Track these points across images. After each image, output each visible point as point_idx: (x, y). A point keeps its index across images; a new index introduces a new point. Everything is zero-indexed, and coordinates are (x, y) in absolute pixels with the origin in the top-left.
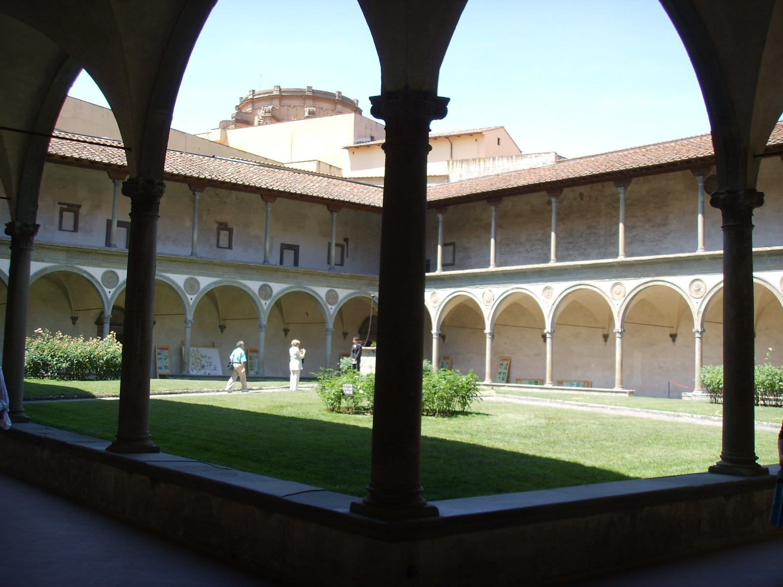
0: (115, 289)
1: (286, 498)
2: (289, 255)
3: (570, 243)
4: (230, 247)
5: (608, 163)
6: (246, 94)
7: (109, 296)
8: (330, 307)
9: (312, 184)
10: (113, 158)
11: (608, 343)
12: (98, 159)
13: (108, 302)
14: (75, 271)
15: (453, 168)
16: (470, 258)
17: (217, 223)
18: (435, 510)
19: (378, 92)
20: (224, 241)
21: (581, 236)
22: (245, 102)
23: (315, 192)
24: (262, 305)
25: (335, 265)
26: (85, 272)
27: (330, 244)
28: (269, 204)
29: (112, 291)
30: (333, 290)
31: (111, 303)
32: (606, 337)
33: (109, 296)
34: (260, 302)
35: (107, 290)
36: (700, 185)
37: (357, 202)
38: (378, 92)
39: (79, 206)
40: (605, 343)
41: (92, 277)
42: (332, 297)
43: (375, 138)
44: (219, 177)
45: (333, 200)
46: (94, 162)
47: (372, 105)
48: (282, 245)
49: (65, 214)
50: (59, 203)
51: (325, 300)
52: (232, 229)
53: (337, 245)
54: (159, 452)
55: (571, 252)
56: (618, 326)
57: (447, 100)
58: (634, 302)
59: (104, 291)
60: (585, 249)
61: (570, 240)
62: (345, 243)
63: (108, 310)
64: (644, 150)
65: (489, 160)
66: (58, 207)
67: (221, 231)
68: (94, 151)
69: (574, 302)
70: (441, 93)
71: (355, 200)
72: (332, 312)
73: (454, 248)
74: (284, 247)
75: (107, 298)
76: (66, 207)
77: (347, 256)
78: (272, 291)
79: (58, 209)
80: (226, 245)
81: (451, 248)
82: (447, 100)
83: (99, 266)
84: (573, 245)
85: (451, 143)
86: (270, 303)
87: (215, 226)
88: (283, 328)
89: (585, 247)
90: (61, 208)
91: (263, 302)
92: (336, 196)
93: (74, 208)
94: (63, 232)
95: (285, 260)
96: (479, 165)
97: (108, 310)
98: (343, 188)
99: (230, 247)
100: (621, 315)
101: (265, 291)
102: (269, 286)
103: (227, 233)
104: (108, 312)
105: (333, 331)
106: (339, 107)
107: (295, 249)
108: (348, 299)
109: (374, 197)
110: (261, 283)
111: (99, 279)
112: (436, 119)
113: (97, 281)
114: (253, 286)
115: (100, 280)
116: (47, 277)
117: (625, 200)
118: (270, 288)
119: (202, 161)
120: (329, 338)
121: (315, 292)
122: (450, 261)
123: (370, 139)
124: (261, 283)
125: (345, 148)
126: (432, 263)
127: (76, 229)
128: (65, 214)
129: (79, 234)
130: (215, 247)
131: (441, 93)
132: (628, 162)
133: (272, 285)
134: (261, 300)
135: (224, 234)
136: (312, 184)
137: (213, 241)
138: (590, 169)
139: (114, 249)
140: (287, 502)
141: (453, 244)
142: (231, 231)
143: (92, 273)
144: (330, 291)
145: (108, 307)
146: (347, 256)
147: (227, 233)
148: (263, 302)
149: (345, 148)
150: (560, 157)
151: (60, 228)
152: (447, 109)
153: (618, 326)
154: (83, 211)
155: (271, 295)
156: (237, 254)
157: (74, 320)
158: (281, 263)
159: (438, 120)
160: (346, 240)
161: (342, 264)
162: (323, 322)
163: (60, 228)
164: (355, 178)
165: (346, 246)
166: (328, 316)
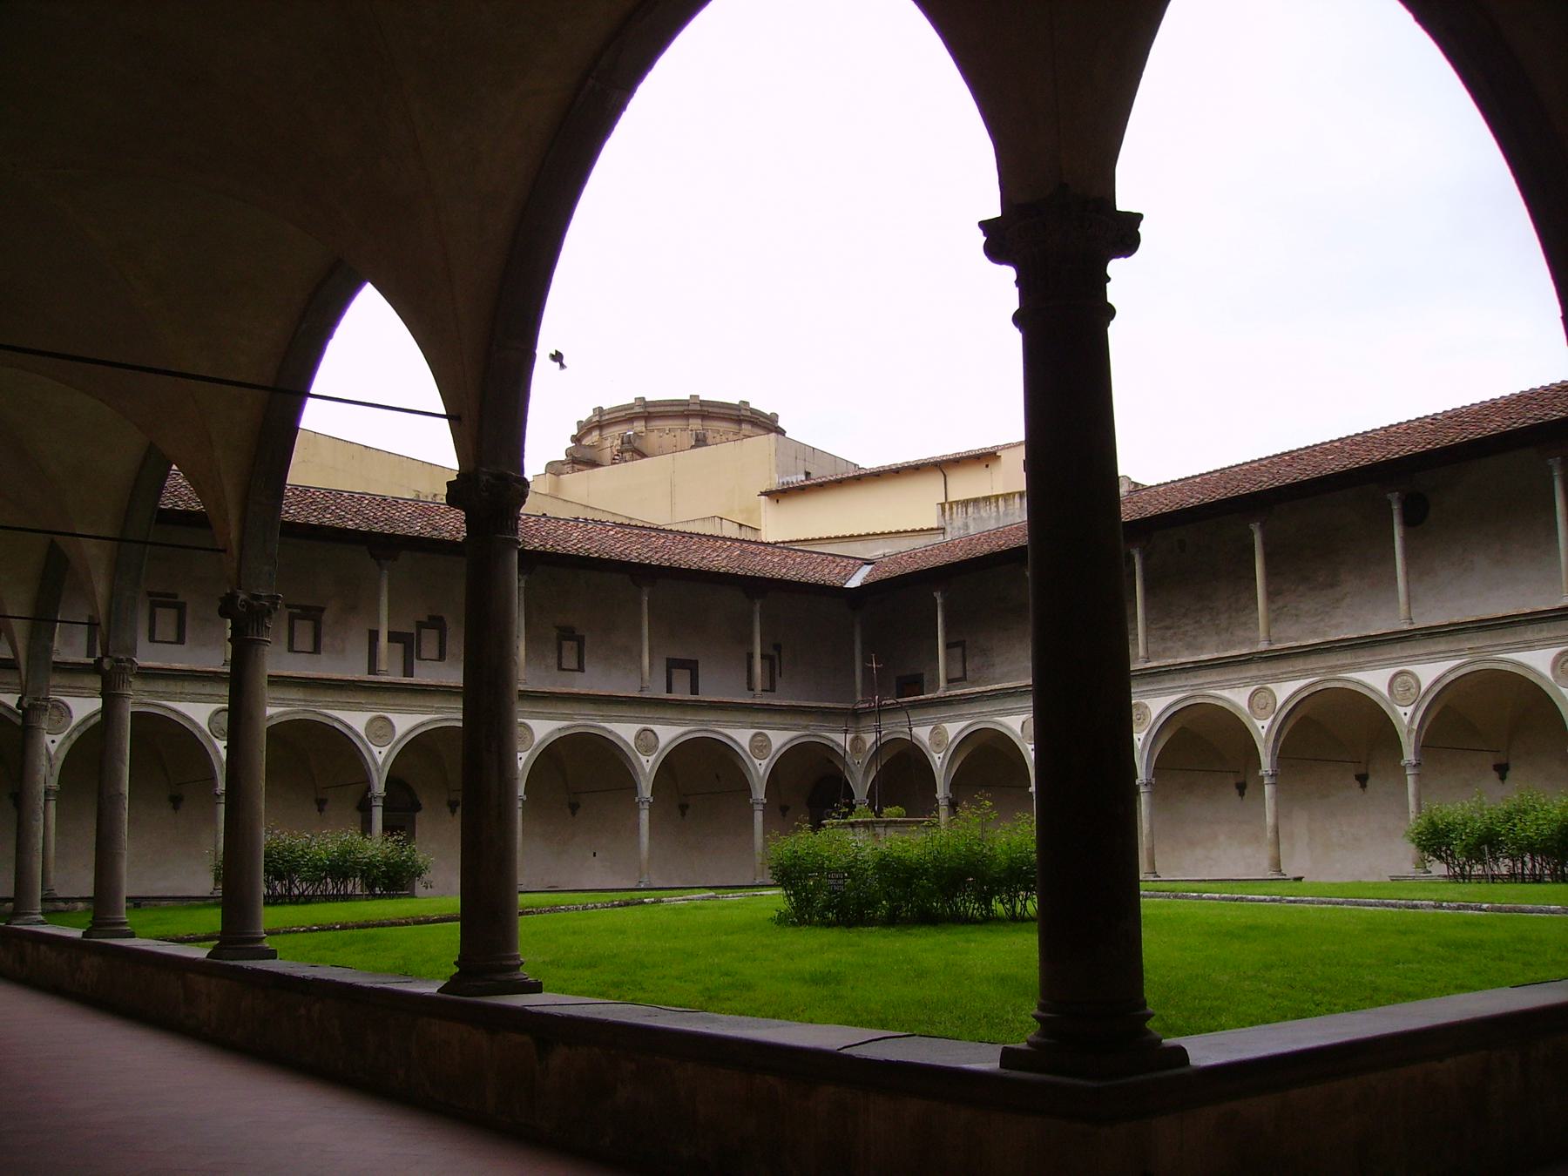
0: (390, 746)
1: (854, 1052)
2: (682, 679)
3: (1168, 628)
4: (581, 669)
5: (1228, 483)
6: (586, 414)
7: (380, 759)
8: (757, 762)
9: (715, 554)
10: (376, 523)
11: (1246, 796)
12: (350, 525)
13: (377, 770)
14: (319, 719)
15: (951, 514)
16: (993, 665)
17: (557, 627)
18: (1180, 1054)
19: (994, 211)
20: (570, 661)
21: (1185, 615)
22: (586, 428)
23: (723, 567)
24: (641, 764)
25: (762, 690)
27: (750, 656)
28: (646, 590)
29: (385, 750)
30: (761, 733)
31: (383, 771)
32: (1241, 788)
33: (380, 759)
34: (638, 758)
35: (375, 750)
36: (1396, 507)
37: (796, 579)
38: (994, 211)
39: (322, 610)
40: (1240, 798)
42: (760, 745)
43: (813, 476)
44: (559, 548)
45: (753, 578)
46: (345, 531)
47: (985, 238)
48: (668, 659)
49: (298, 623)
51: (748, 749)
52: (583, 637)
53: (763, 657)
54: (541, 992)
55: (1170, 644)
56: (1266, 763)
57: (1136, 218)
58: (1291, 723)
59: (368, 749)
60: (1195, 637)
61: (1168, 622)
62: (776, 653)
63: (379, 783)
64: (1287, 458)
65: (1014, 498)
67: (564, 642)
68: (343, 513)
69: (1183, 730)
70: (1121, 205)
71: (792, 575)
72: (761, 771)
73: (964, 651)
74: (673, 665)
75: (376, 762)
77: (780, 676)
78: (657, 738)
80: (575, 666)
81: (958, 651)
82: (1136, 218)
83: (359, 708)
84: (1172, 631)
85: (945, 476)
86: (656, 760)
87: (554, 633)
89: (1194, 633)
90: (290, 613)
91: (643, 759)
92: (759, 571)
93: (313, 614)
94: (297, 655)
95: (675, 687)
96: (997, 506)
97: (379, 783)
98: (769, 558)
99: (581, 669)
100: (1270, 744)
101: (646, 740)
102: (652, 731)
103: (574, 644)
104: (379, 787)
105: (763, 803)
106: (746, 428)
107: (692, 667)
108: (789, 746)
109: (822, 571)
110: (639, 727)
111: (361, 729)
112: (1118, 256)
113: (358, 735)
114: (625, 731)
115: (363, 734)
117: (1265, 544)
118: (655, 734)
119: (527, 523)
120: (759, 816)
121: (731, 739)
122: (958, 674)
123: (804, 478)
124: (639, 727)
125: (762, 494)
126: (926, 678)
127: (316, 650)
128: (298, 623)
129: (323, 656)
130: (556, 670)
131: (1121, 205)
132: (1265, 479)
133: (656, 728)
135: (569, 646)
136: (715, 554)
137: (553, 661)
138: (1198, 496)
139: (383, 679)
140: (850, 1058)
141: (962, 644)
142: (580, 642)
143: (349, 722)
144: (755, 735)
145: (379, 778)
146: (780, 676)
147: (574, 644)
148: (643, 759)
149: (762, 494)
150: (1136, 484)
152: (1138, 235)
153: (1266, 763)
154: (327, 617)
155: (656, 746)
156: (592, 681)
158: (669, 690)
159: (1122, 259)
160: (777, 647)
161: (772, 689)
162: (746, 789)
163: (291, 649)
164: (783, 542)
165: (777, 656)
166: (756, 779)
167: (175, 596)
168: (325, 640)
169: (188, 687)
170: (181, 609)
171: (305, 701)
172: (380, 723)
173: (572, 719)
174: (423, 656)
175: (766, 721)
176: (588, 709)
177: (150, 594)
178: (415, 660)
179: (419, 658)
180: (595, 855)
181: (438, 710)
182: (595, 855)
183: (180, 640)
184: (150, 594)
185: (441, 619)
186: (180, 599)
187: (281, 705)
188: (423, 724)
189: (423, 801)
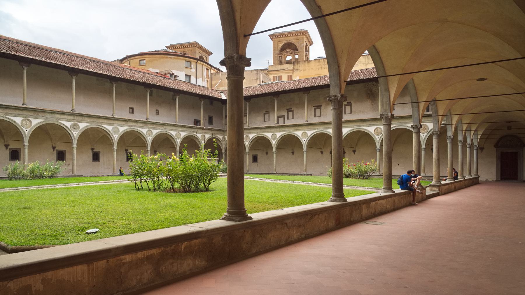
7: (304, 142)
26: (295, 134)
39: (321, 106)
41: (298, 135)
50: (314, 107)
59: (302, 140)
66: (313, 108)
76: (316, 107)
79: (314, 108)
83: (300, 130)
88: (352, 150)
90: (314, 108)
91: (377, 137)
110: (375, 127)
116: (350, 135)
124: (375, 127)
129: (322, 117)
134: (376, 136)
151: (315, 116)
154: (322, 108)
157: (322, 152)
163: (315, 116)
167: (291, 109)
168: (322, 113)
169: (267, 130)
170: (293, 111)
171: (288, 130)
172: (304, 134)
173: (354, 127)
174: (346, 113)
175: (426, 120)
176: (358, 124)
177: (287, 109)
178: (344, 115)
179: (345, 114)
180: (398, 165)
181: (317, 129)
182: (398, 165)
183: (293, 118)
184: (287, 109)
185: (351, 102)
186: (292, 109)
187: (284, 132)
188: (314, 133)
189: (346, 150)
